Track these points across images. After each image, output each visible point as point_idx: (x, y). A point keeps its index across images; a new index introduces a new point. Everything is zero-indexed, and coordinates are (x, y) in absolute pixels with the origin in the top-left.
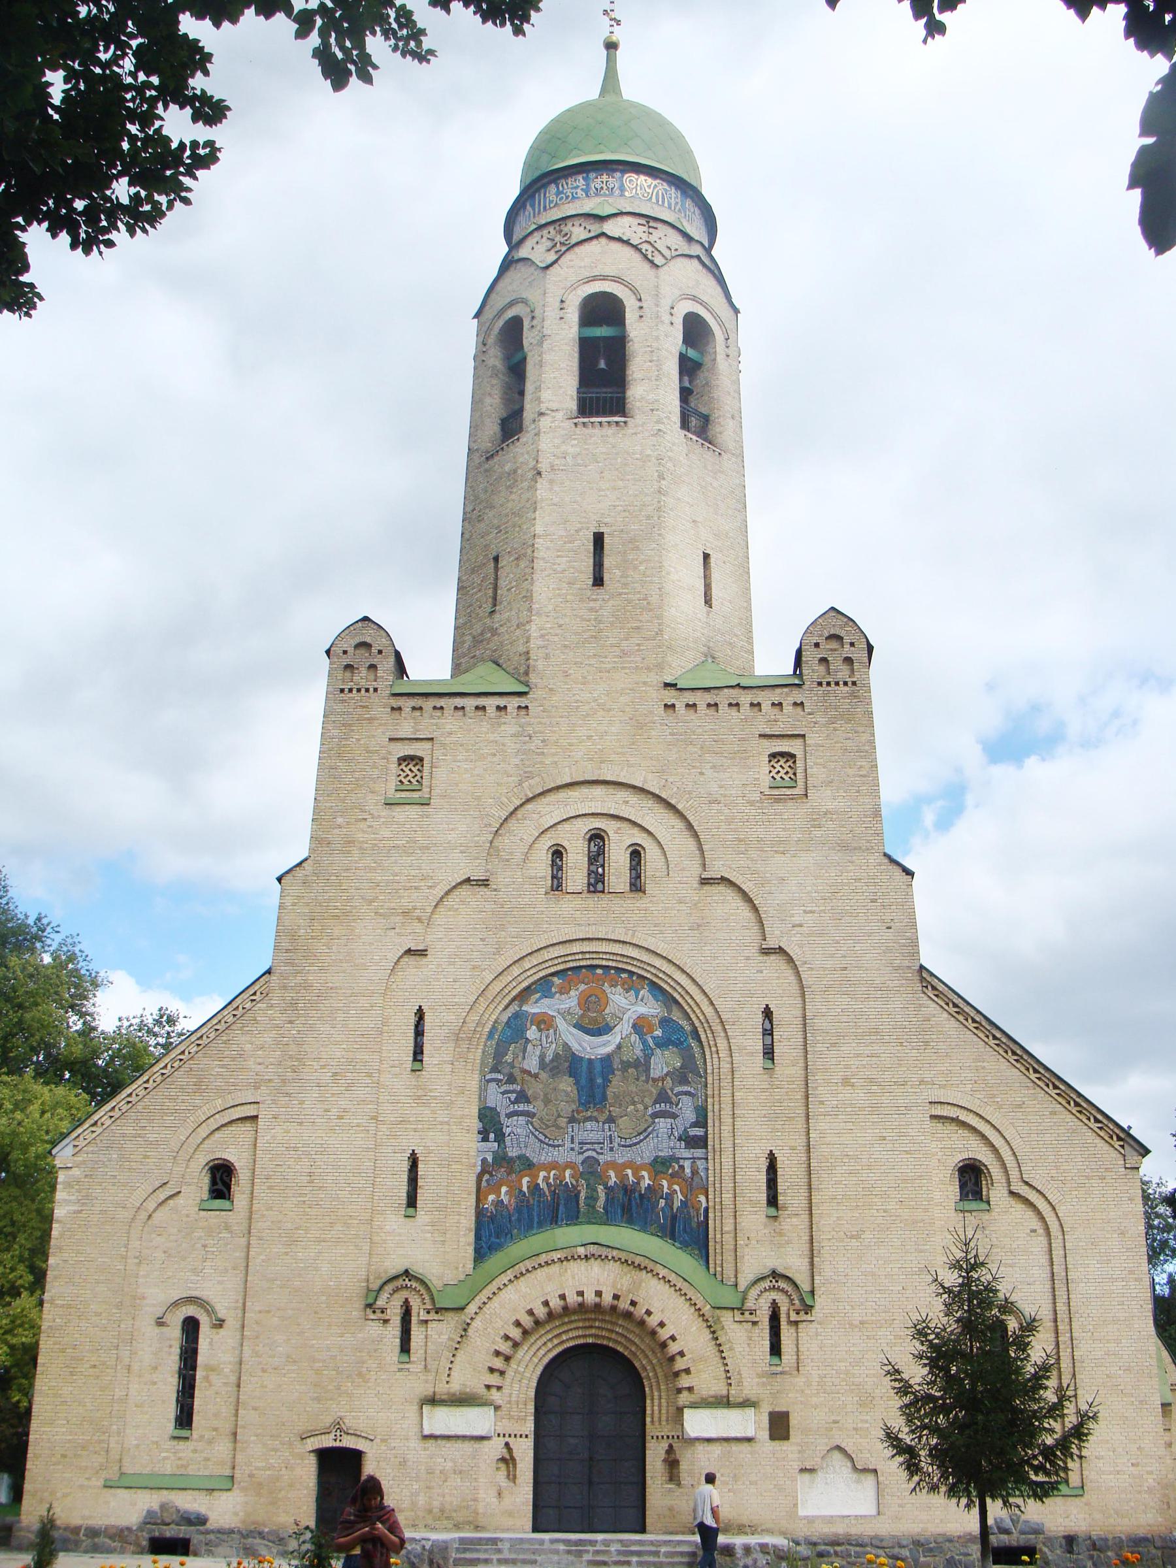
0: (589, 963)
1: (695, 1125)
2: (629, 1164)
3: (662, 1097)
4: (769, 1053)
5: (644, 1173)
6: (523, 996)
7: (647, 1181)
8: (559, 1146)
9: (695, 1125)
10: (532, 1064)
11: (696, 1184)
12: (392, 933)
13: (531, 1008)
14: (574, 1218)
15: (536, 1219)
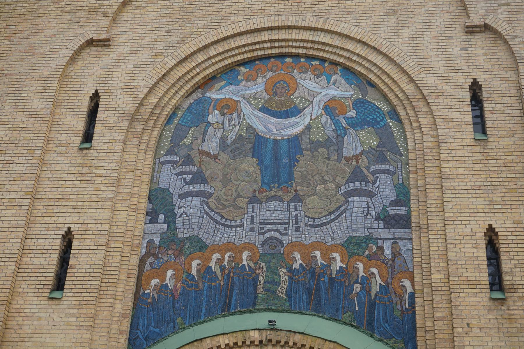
0: (277, 51)
1: (393, 203)
2: (319, 245)
3: (357, 175)
4: (480, 123)
5: (335, 255)
6: (209, 82)
7: (339, 264)
8: (236, 227)
9: (393, 203)
10: (212, 145)
11: (397, 267)
12: (76, 26)
13: (215, 94)
14: (250, 306)
15: (204, 305)
